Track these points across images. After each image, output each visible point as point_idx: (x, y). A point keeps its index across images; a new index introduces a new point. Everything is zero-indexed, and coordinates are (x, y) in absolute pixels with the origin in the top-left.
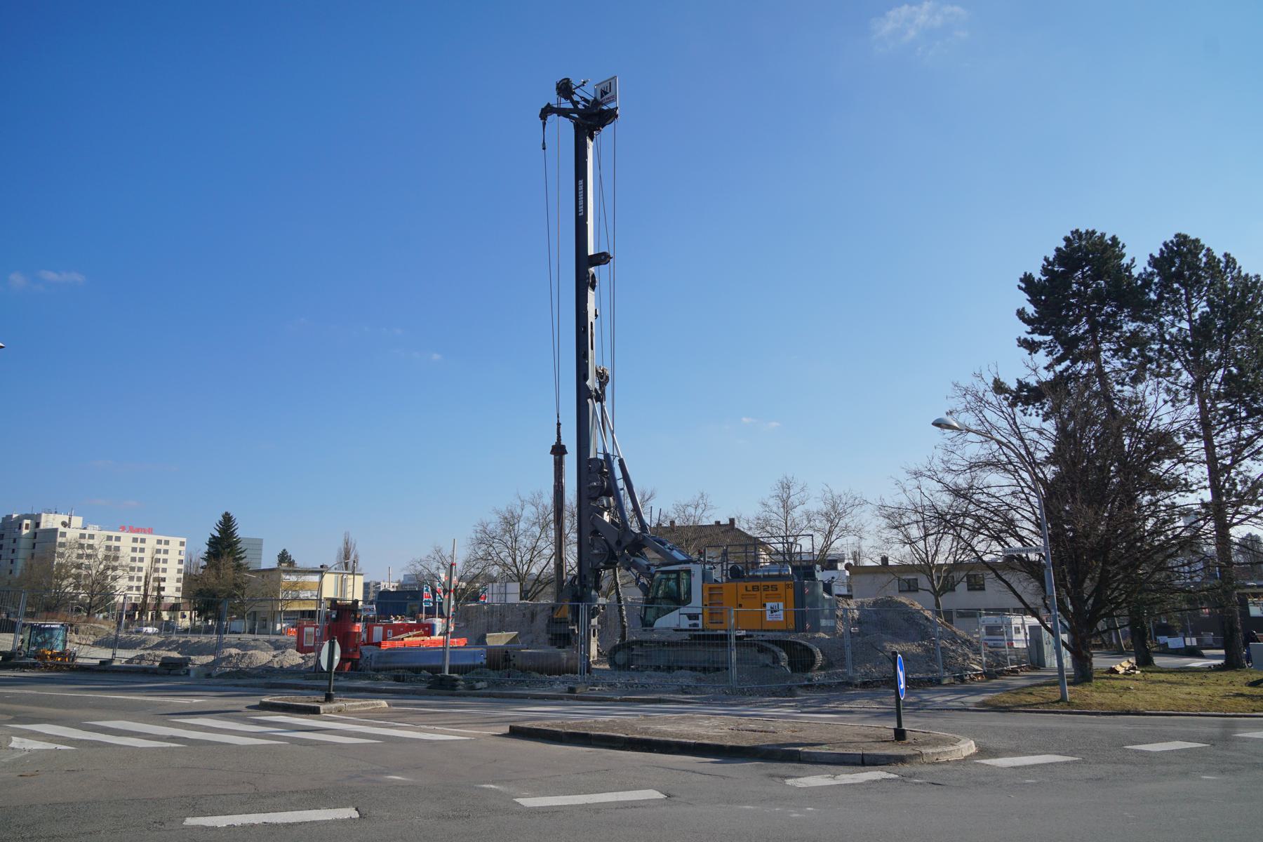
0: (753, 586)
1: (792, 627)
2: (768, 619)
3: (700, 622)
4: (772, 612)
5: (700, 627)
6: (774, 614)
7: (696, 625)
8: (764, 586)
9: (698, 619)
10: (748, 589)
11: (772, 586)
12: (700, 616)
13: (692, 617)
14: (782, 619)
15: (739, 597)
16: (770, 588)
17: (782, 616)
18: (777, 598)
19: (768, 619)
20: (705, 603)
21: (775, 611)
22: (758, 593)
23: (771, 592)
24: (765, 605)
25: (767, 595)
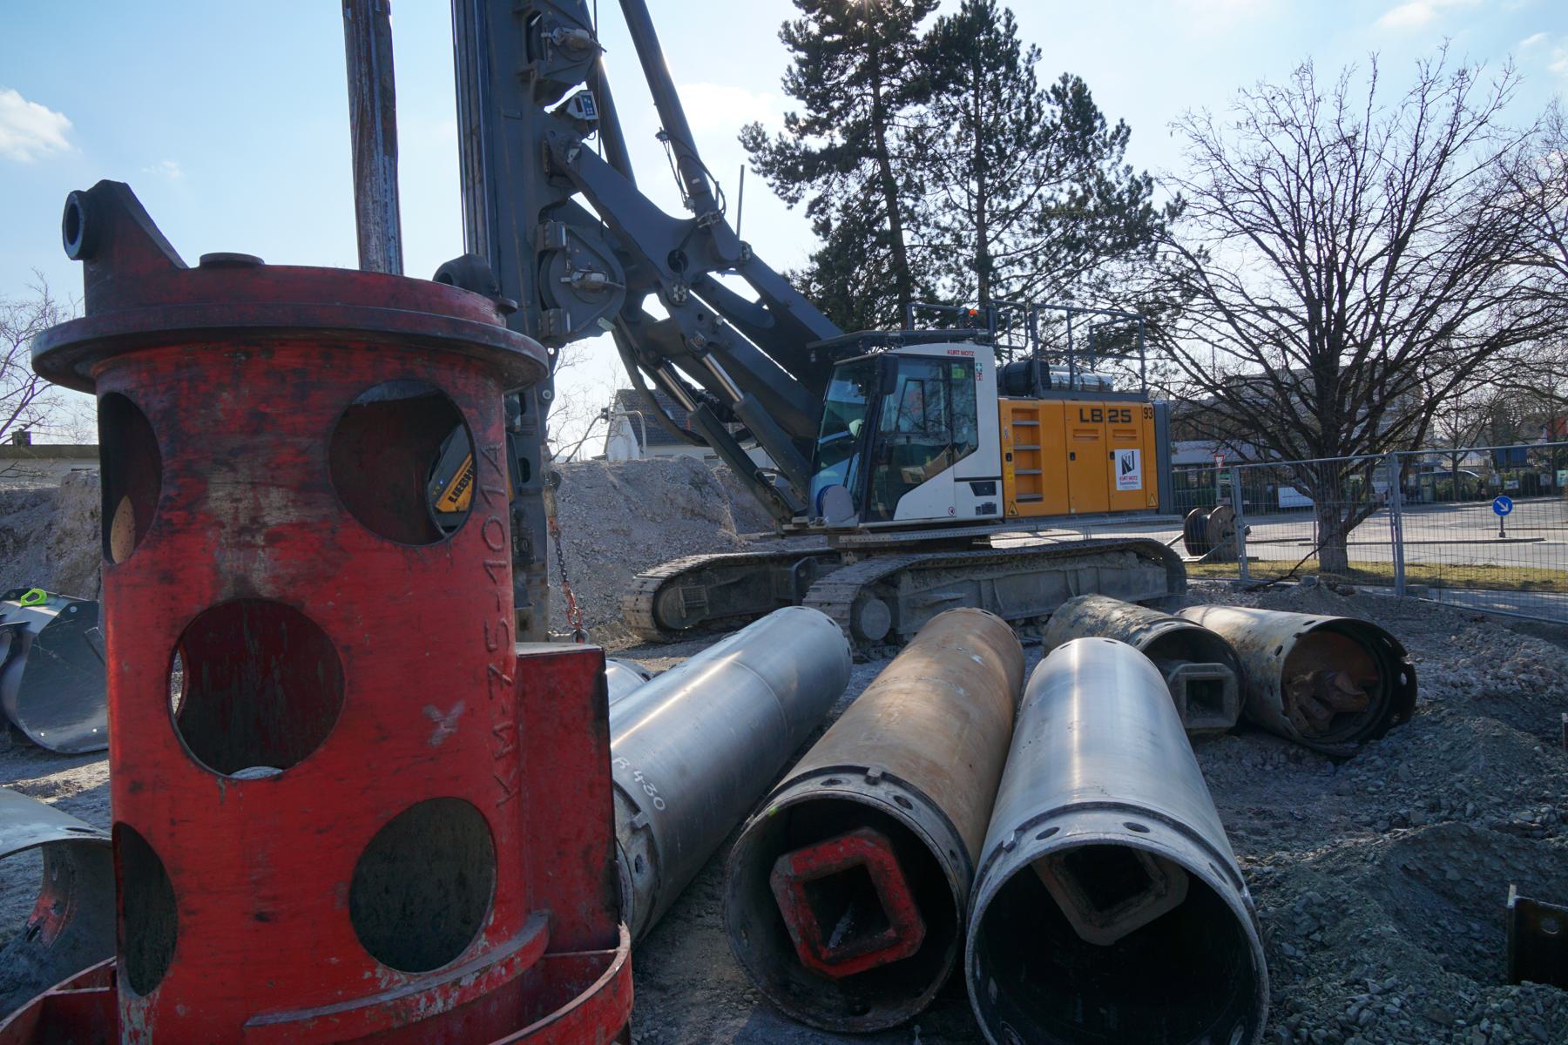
0: (1093, 411)
1: (1154, 503)
2: (1119, 488)
3: (996, 499)
4: (1124, 472)
5: (1000, 513)
6: (1128, 474)
7: (990, 508)
8: (1110, 411)
9: (993, 492)
10: (1085, 417)
11: (1122, 411)
12: (998, 483)
13: (982, 486)
14: (1139, 486)
15: (1070, 436)
16: (1120, 418)
17: (1139, 480)
18: (1131, 439)
19: (1119, 488)
20: (1007, 450)
21: (1130, 470)
22: (1100, 426)
23: (1121, 426)
24: (1112, 455)
25: (1114, 431)
